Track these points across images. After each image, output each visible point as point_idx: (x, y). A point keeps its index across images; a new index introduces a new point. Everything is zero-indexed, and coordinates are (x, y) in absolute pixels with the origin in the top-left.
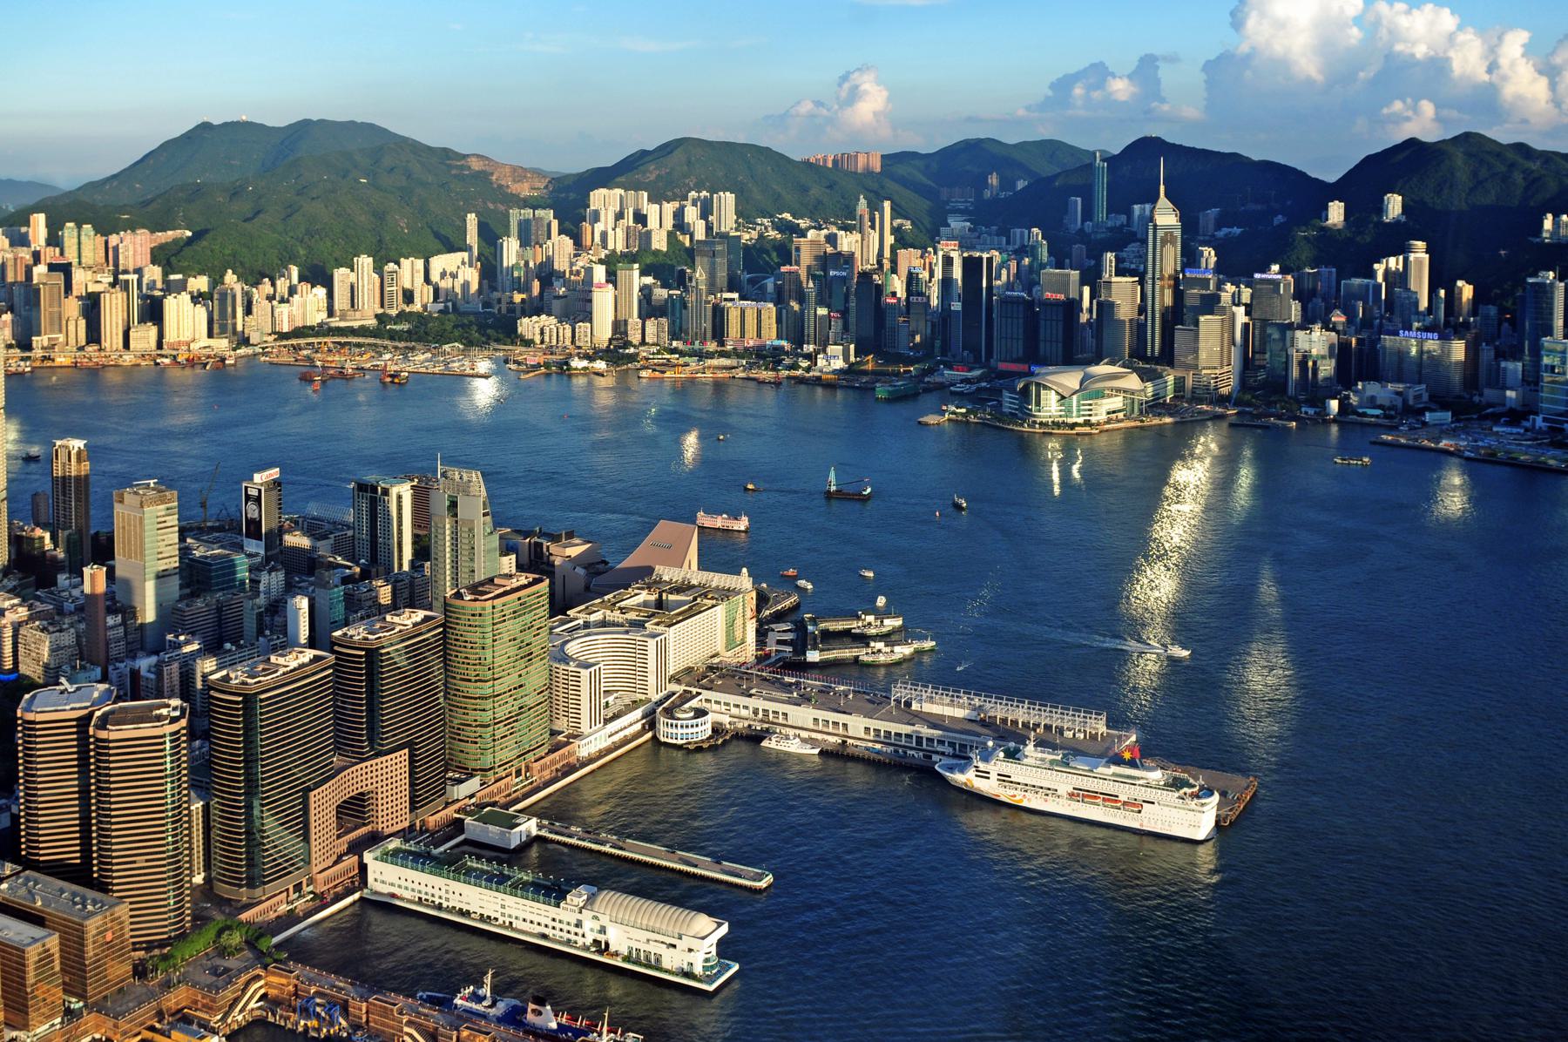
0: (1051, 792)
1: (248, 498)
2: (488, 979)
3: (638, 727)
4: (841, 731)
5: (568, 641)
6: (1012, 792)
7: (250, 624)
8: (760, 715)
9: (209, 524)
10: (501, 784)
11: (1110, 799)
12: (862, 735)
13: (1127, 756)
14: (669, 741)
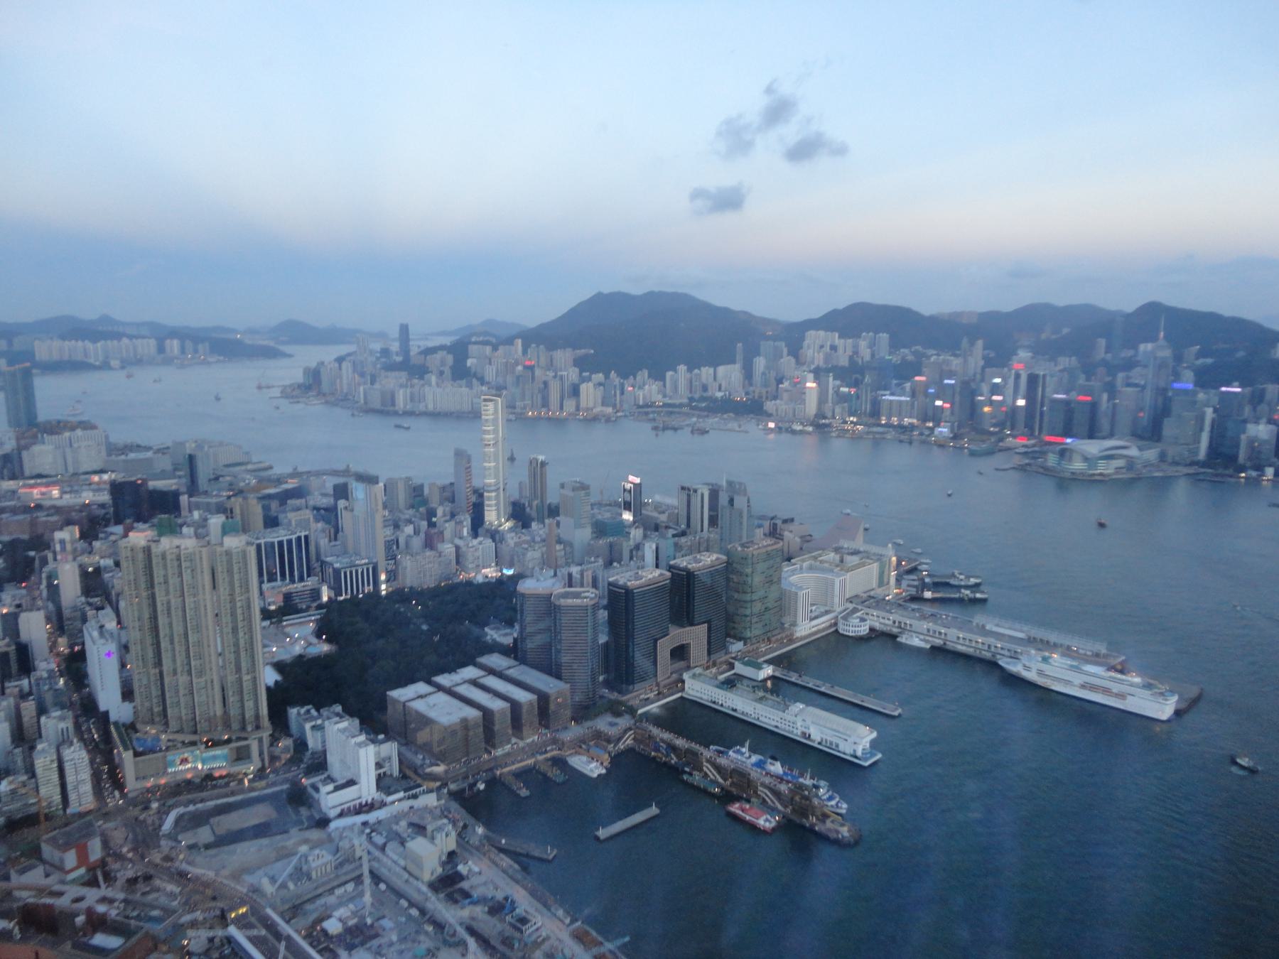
0: (1068, 682)
1: (625, 490)
2: (747, 744)
3: (828, 624)
4: (943, 636)
5: (790, 576)
6: (1046, 680)
7: (626, 555)
8: (897, 624)
9: (604, 502)
10: (755, 646)
11: (1106, 691)
12: (955, 640)
13: (1119, 667)
14: (845, 633)
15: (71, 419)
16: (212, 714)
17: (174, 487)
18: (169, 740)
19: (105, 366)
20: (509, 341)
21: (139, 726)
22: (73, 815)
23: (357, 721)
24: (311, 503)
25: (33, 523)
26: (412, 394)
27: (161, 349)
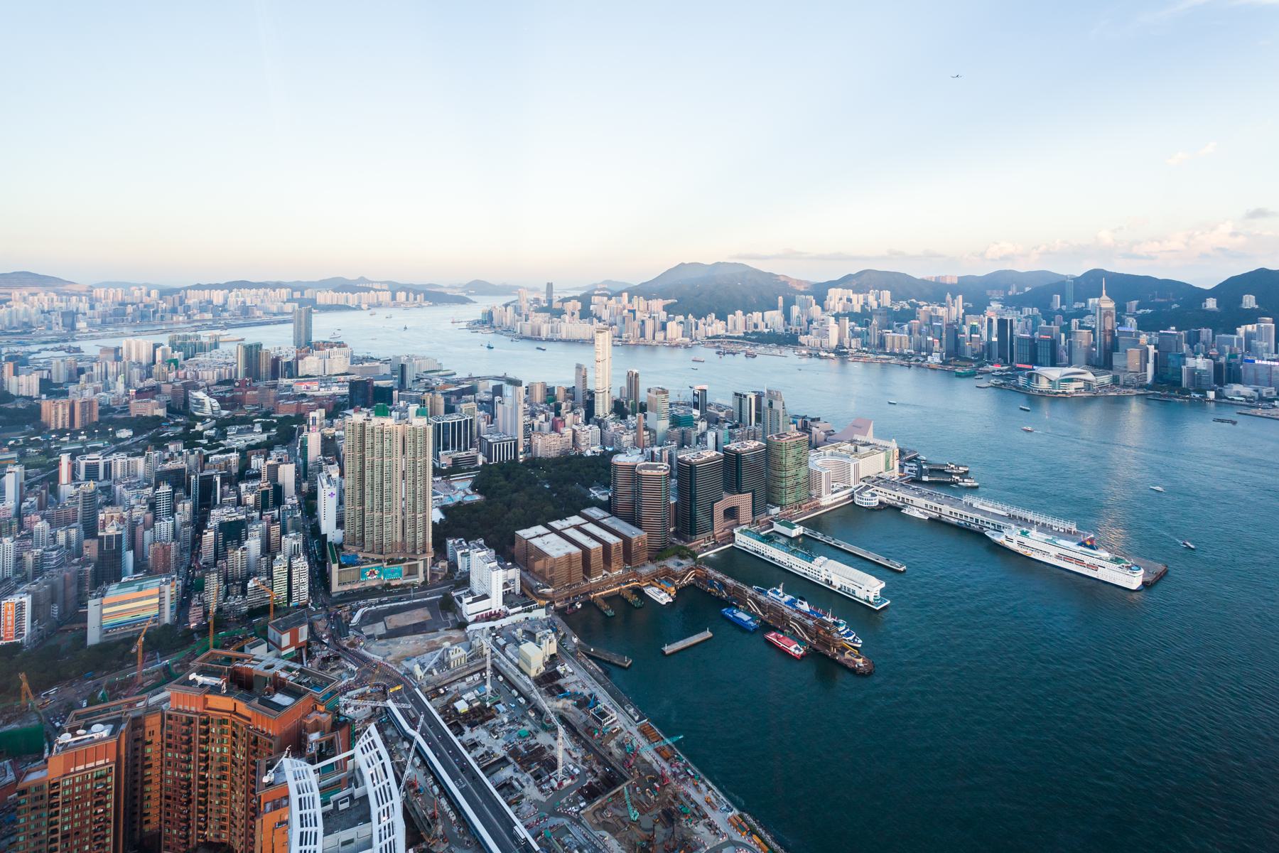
0: (1045, 553)
3: (846, 497)
7: (694, 440)
10: (789, 511)
11: (1080, 562)
15: (331, 340)
16: (394, 541)
17: (390, 385)
18: (364, 558)
19: (358, 308)
20: (619, 294)
21: (345, 546)
22: (293, 607)
23: (493, 552)
24: (478, 398)
25: (299, 406)
26: (552, 327)
27: (394, 298)
